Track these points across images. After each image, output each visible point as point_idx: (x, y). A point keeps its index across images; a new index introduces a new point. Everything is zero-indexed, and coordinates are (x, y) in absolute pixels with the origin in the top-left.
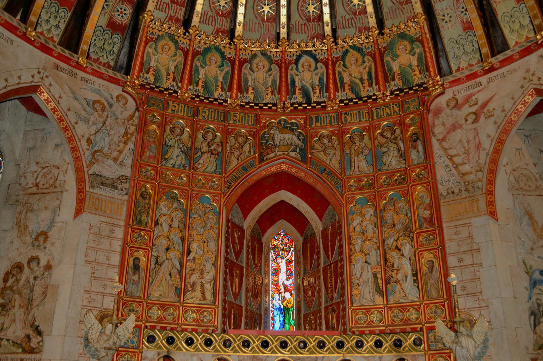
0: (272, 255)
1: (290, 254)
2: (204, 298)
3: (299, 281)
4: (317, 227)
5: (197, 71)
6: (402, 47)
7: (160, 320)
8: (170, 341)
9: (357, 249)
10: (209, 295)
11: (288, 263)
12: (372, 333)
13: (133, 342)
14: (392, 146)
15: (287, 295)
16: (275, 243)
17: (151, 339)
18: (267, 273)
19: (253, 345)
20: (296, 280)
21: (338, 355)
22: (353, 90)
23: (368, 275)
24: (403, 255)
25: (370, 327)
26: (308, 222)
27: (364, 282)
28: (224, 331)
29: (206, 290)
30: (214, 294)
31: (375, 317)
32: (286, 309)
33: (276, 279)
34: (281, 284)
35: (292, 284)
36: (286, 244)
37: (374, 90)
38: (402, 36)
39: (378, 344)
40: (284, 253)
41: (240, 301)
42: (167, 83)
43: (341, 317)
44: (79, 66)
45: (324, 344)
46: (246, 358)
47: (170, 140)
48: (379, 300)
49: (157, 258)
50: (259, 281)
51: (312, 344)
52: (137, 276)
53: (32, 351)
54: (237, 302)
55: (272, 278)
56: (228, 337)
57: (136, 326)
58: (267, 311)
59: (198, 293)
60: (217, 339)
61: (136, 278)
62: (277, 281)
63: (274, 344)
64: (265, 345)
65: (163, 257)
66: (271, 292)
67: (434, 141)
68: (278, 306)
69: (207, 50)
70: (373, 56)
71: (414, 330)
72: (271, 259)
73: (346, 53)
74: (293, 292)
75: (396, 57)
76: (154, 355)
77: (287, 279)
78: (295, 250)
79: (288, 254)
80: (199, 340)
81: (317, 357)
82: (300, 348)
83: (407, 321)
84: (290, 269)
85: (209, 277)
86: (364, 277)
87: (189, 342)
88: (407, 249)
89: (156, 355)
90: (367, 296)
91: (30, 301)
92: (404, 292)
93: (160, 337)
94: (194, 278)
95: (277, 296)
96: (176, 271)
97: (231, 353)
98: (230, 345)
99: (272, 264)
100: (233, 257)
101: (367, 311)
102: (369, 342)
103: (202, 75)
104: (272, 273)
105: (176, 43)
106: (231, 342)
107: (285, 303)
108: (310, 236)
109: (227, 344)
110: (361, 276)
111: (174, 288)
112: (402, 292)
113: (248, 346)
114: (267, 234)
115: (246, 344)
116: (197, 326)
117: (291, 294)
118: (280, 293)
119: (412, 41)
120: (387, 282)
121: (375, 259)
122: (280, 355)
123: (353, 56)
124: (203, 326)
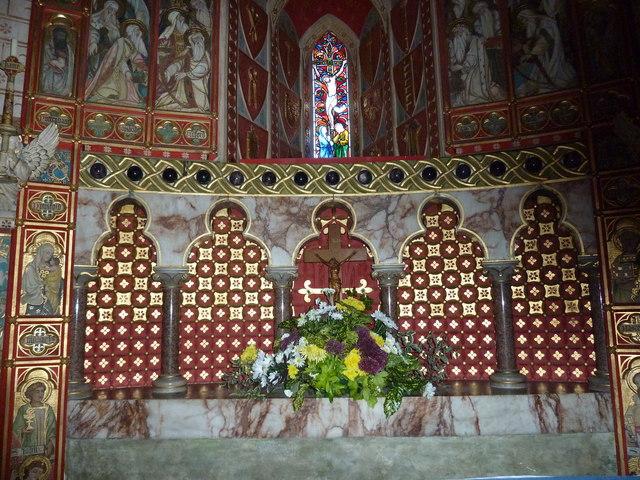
0: (315, 72)
1: (342, 70)
2: (192, 103)
3: (357, 104)
4: (383, 8)
9: (458, 12)
10: (201, 99)
11: (340, 82)
13: (60, 175)
15: (339, 128)
16: (319, 54)
18: (308, 98)
19: (280, 180)
20: (351, 105)
21: (425, 191)
23: (478, 54)
24: (544, 13)
25: (483, 140)
26: (372, 5)
27: (474, 67)
28: (232, 160)
29: (196, 91)
30: (212, 97)
33: (322, 105)
34: (329, 112)
35: (346, 111)
36: (336, 54)
40: (333, 68)
41: (264, 123)
45: (402, 174)
46: (269, 201)
49: (103, 32)
52: (62, 61)
54: (257, 122)
56: (236, 168)
57: (61, 146)
59: (181, 95)
60: (221, 172)
61: (60, 63)
62: (324, 108)
63: (316, 176)
64: (301, 179)
65: (114, 32)
66: (315, 125)
68: (326, 143)
72: (314, 77)
74: (348, 123)
76: (105, 197)
77: (338, 105)
78: (350, 64)
79: (338, 70)
81: (390, 197)
82: (362, 183)
84: (343, 91)
86: (471, 59)
89: (109, 197)
90: (477, 90)
92: (546, 76)
94: (172, 70)
95: (324, 130)
96: (139, 57)
97: (244, 194)
98: (241, 182)
99: (315, 85)
100: (246, 48)
104: (316, 97)
106: (242, 176)
107: (335, 139)
108: (372, 29)
109: (236, 179)
110: (465, 57)
111: (136, 85)
112: (542, 76)
113: (273, 182)
114: (307, 36)
115: (269, 178)
116: (181, 148)
117: (345, 126)
118: (328, 125)
121: (490, 27)
122: (326, 194)
124: (191, 148)
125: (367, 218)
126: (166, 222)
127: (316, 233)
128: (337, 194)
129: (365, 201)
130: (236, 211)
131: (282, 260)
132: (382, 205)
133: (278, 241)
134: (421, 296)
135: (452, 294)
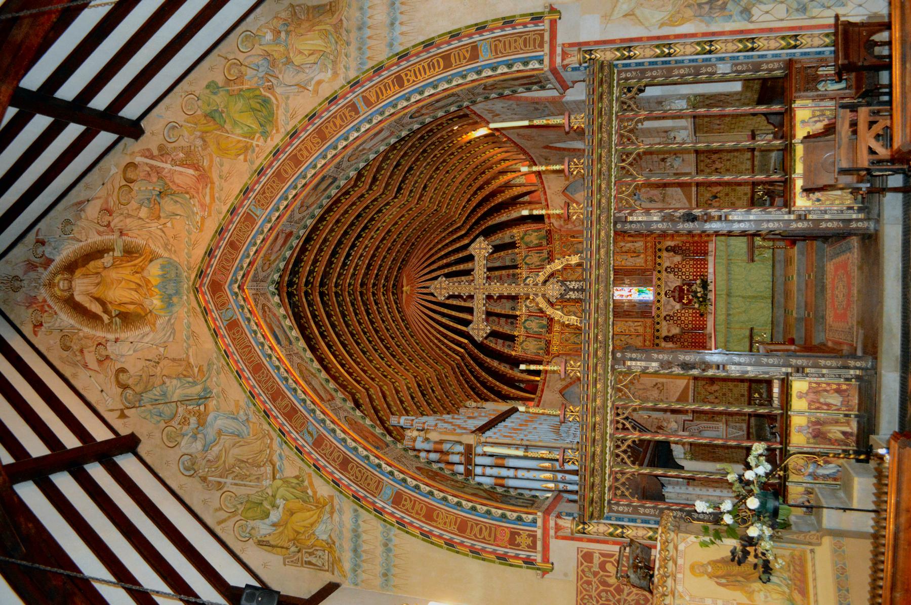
5: (536, 332)
6: (527, 239)
7: (650, 341)
8: (658, 338)
10: (639, 324)
12: (655, 260)
14: (576, 246)
17: (657, 345)
22: (544, 261)
23: (631, 260)
31: (649, 258)
32: (639, 291)
37: (545, 252)
38: (522, 238)
39: (660, 257)
42: (543, 344)
43: (648, 270)
44: (545, 379)
47: (572, 340)
48: (642, 256)
50: (626, 304)
51: (659, 283)
53: (663, 386)
55: (624, 298)
58: (640, 300)
59: (639, 328)
60: (657, 320)
63: (659, 298)
64: (659, 301)
65: (624, 342)
67: (575, 229)
69: (525, 328)
70: (529, 251)
71: (655, 244)
73: (526, 263)
75: (531, 242)
80: (658, 327)
83: (651, 247)
85: (631, 324)
87: (658, 331)
88: (622, 244)
91: (644, 389)
93: (657, 341)
101: (646, 261)
102: (658, 261)
103: (537, 330)
105: (523, 341)
109: (658, 316)
119: (526, 234)
120: (635, 252)
123: (527, 260)
125: (669, 287)
126: (669, 331)
127: (672, 299)
128: (663, 293)
129: (665, 286)
130: (665, 318)
131: (678, 306)
132: (666, 282)
133: (673, 307)
134: (687, 274)
135: (688, 266)
